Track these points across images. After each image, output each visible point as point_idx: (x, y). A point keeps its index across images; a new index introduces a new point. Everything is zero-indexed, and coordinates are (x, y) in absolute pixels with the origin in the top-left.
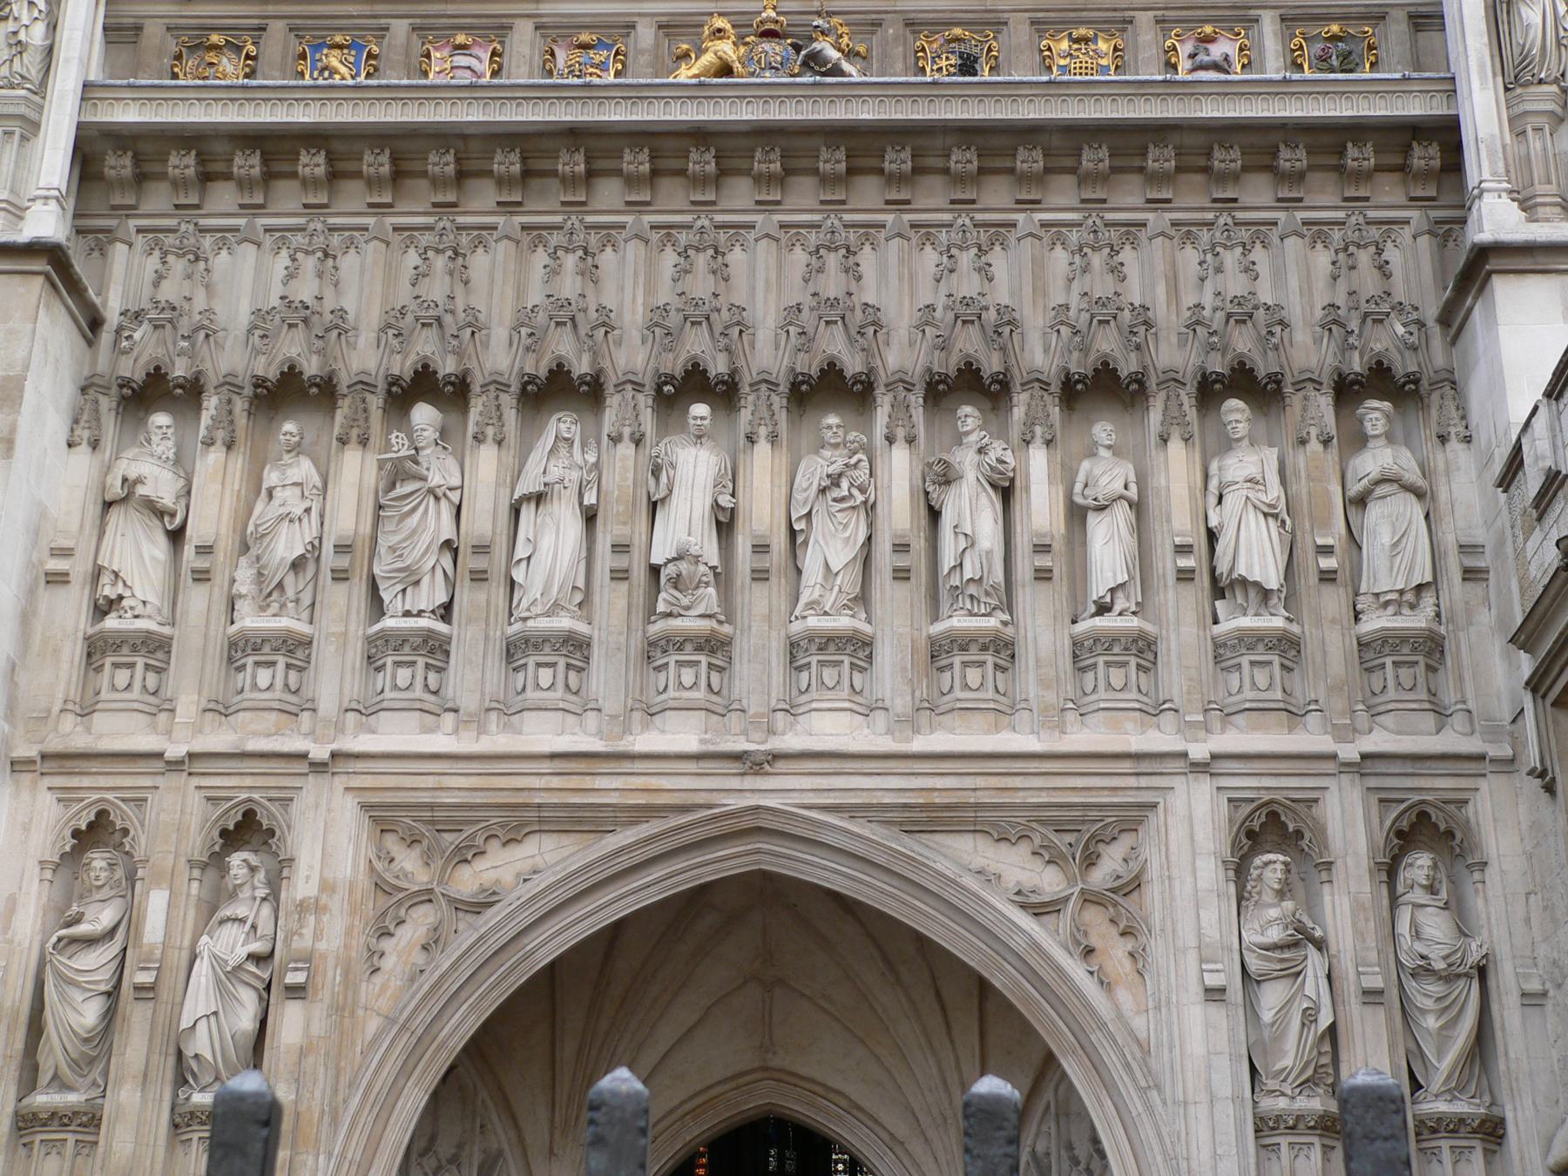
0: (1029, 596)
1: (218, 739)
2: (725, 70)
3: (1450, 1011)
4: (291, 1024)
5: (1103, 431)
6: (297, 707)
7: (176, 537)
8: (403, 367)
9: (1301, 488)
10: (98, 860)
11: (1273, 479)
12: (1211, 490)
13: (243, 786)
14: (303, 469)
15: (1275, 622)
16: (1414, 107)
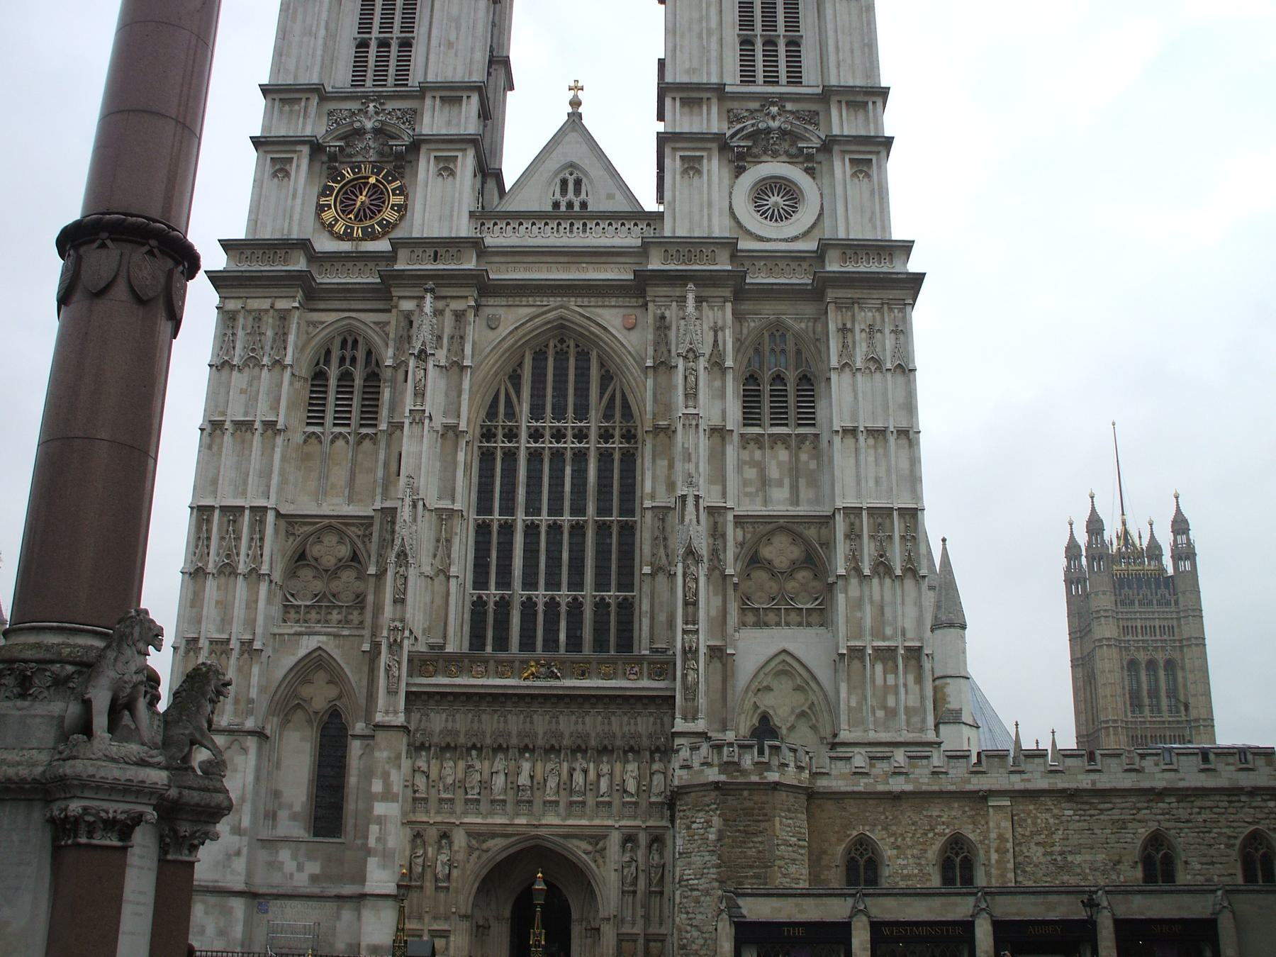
0: (588, 793)
1: (439, 819)
2: (533, 674)
3: (656, 873)
4: (455, 873)
5: (605, 759)
6: (452, 813)
7: (428, 777)
8: (469, 745)
9: (642, 771)
10: (419, 841)
11: (636, 770)
12: (624, 771)
13: (444, 828)
14: (451, 763)
15: (634, 800)
16: (668, 693)
